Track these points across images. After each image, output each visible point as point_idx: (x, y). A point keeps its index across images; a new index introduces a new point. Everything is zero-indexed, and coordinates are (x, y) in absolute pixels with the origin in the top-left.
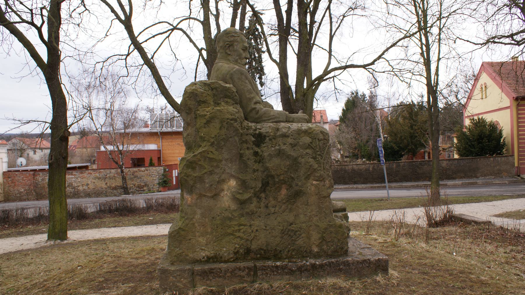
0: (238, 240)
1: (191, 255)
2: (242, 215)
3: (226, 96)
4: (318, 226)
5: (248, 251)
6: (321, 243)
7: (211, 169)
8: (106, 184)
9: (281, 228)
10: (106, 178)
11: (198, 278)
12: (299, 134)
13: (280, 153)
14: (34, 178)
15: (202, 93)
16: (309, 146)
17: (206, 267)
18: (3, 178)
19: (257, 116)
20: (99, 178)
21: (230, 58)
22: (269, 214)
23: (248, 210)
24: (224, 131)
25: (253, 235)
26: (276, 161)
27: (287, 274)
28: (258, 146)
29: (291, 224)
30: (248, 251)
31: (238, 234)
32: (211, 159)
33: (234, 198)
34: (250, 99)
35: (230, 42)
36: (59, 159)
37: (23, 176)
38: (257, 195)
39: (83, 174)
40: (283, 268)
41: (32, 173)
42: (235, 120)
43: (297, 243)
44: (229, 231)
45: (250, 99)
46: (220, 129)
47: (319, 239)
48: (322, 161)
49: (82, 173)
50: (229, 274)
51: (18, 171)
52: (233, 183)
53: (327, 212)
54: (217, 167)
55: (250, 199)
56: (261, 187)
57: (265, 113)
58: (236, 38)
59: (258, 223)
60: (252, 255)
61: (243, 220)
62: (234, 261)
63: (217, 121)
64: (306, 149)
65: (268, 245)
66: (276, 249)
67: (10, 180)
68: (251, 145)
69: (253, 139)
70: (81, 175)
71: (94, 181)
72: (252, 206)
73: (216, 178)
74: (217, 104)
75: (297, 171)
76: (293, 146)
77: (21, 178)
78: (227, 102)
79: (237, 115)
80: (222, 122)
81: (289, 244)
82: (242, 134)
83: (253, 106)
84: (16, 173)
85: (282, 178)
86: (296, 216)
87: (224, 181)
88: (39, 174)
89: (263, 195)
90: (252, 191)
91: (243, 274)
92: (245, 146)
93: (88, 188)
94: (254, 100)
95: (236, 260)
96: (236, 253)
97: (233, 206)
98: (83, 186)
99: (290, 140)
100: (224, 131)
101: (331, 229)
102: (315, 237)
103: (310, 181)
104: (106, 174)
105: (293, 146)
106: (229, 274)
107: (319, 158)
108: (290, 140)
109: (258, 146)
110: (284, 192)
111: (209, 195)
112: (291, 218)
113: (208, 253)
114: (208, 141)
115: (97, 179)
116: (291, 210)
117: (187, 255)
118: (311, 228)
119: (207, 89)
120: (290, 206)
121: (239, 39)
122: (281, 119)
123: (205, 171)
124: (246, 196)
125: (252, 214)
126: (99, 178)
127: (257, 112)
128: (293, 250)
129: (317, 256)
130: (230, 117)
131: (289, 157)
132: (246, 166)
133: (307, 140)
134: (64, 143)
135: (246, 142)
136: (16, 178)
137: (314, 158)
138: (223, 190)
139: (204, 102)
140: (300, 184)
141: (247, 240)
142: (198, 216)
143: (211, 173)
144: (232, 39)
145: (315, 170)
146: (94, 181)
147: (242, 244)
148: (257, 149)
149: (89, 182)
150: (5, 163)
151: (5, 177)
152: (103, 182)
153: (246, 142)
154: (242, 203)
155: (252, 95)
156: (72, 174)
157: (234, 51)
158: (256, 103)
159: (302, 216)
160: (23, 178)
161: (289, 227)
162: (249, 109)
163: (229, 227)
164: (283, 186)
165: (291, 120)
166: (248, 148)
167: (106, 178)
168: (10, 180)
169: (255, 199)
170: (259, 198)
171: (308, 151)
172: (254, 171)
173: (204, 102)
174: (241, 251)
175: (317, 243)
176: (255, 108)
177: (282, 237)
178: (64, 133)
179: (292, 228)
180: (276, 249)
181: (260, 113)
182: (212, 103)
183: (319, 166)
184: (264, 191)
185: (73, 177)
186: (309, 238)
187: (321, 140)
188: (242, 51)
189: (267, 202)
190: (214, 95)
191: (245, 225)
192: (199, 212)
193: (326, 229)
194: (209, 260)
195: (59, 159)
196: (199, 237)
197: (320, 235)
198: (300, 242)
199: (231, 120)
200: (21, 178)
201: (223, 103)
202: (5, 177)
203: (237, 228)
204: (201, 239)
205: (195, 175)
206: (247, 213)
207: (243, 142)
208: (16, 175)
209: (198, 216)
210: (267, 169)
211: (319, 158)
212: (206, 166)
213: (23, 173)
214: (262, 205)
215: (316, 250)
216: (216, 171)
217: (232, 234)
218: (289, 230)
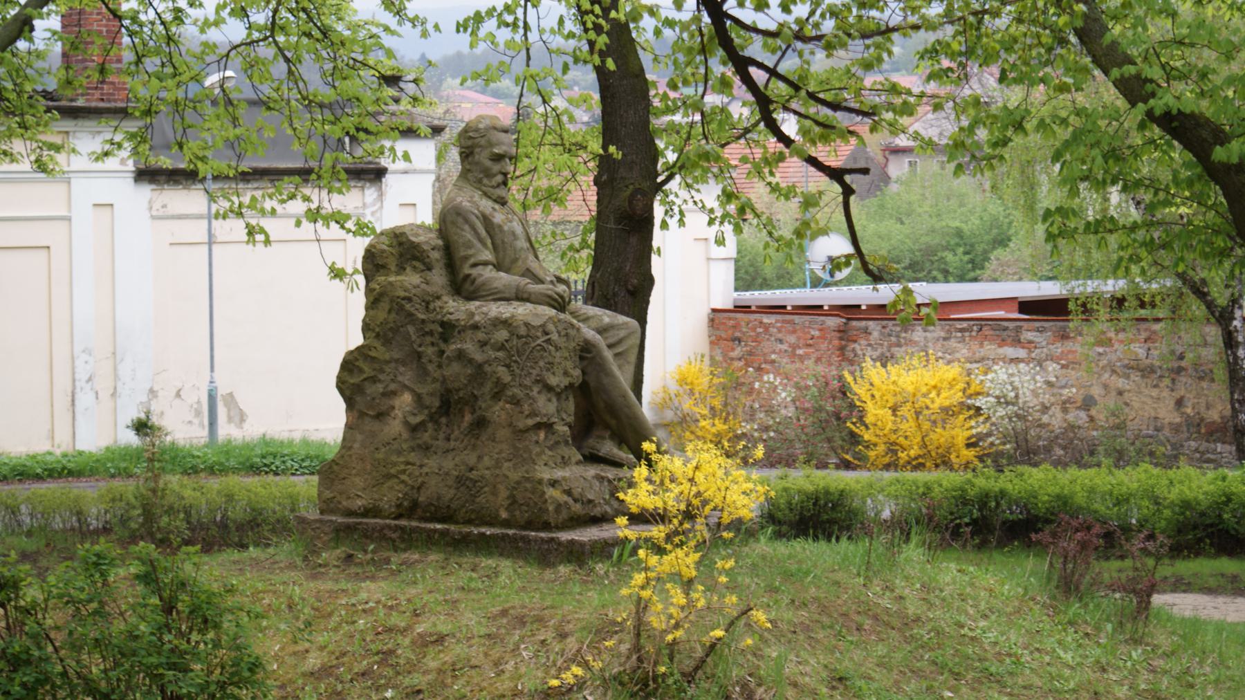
0: (402, 486)
1: (344, 503)
2: (413, 450)
3: (415, 258)
4: (507, 477)
5: (415, 505)
6: (510, 505)
7: (372, 374)
8: (1179, 403)
9: (456, 473)
10: (1180, 370)
11: (342, 534)
12: (495, 326)
13: (461, 355)
14: (842, 349)
15: (383, 251)
16: (502, 347)
17: (352, 520)
18: (712, 343)
19: (472, 288)
20: (1147, 371)
21: (470, 175)
22: (448, 451)
23: (420, 442)
24: (393, 315)
25: (420, 480)
26: (456, 367)
27: (448, 544)
28: (446, 341)
29: (471, 469)
30: (415, 505)
31: (404, 477)
32: (373, 359)
33: (406, 423)
34: (466, 258)
35: (467, 148)
36: (615, 295)
37: (792, 339)
38: (433, 418)
39: (1069, 345)
40: (444, 533)
41: (833, 322)
42: (409, 299)
43: (478, 500)
44: (393, 471)
45: (466, 258)
46: (390, 312)
47: (508, 498)
48: (517, 371)
49: (1064, 337)
50: (376, 534)
51: (778, 309)
52: (407, 398)
53: (525, 456)
54: (382, 371)
55: (422, 423)
56: (440, 407)
57: (484, 284)
58: (477, 141)
59: (432, 463)
60: (419, 511)
61: (413, 457)
62: (395, 518)
63: (387, 299)
64: (499, 350)
65: (439, 498)
66: (448, 507)
67: (737, 352)
68: (435, 339)
69: (440, 330)
70: (1058, 348)
71: (1121, 383)
72: (426, 437)
73: (380, 388)
74: (401, 269)
75: (482, 384)
76: (483, 344)
77: (784, 347)
78: (415, 267)
79: (414, 291)
80: (392, 301)
81: (467, 501)
82: (423, 321)
83: (467, 270)
84: (767, 319)
85: (461, 394)
86: (480, 458)
87: (394, 393)
88: (866, 331)
89: (444, 420)
90: (426, 412)
91: (394, 536)
92: (428, 339)
93: (1092, 419)
94: (472, 261)
95: (399, 517)
96: (399, 506)
97: (405, 435)
98: (1065, 410)
99: (481, 335)
100: (393, 315)
101: (528, 485)
102: (503, 493)
103: (501, 404)
104: (1179, 349)
105: (483, 344)
106: (376, 534)
107: (515, 366)
108: (481, 335)
109: (446, 341)
110: (468, 418)
111: (371, 413)
112: (472, 460)
113: (364, 502)
114: (373, 330)
115: (1137, 377)
116: (474, 447)
117: (340, 503)
118: (499, 480)
119: (395, 243)
120: (473, 441)
121: (483, 142)
122: (507, 295)
123: (365, 376)
124: (418, 419)
125: (426, 449)
126: (1147, 371)
127: (473, 282)
128: (473, 511)
129: (507, 524)
130: (402, 294)
131: (471, 361)
132: (426, 373)
133: (502, 335)
134: (634, 240)
135: (431, 333)
136: (767, 346)
137: (508, 366)
138: (393, 408)
139: (383, 267)
140: (483, 406)
141: (413, 488)
142: (356, 445)
143: (373, 380)
144: (470, 143)
145: (505, 386)
146: (1121, 383)
147: (406, 494)
148: (443, 346)
149: (1096, 391)
150: (723, 264)
151: (720, 338)
152: (1166, 393)
153: (431, 333)
154: (414, 429)
155: (470, 252)
156: (1017, 342)
157: (477, 163)
158: (475, 265)
159: (486, 459)
160: (794, 347)
161: (468, 474)
162: (461, 276)
163: (395, 464)
164: (467, 409)
165: (525, 296)
166: (433, 344)
167: (1180, 370)
168: (737, 352)
169: (430, 425)
170: (436, 422)
171: (500, 354)
172: (435, 380)
173: (383, 267)
174: (406, 504)
175: (506, 503)
176: (468, 276)
177: (457, 489)
178: (630, 202)
179: (474, 475)
180: (448, 507)
181: (479, 281)
182: (393, 268)
183: (513, 380)
184: (447, 414)
185: (1022, 353)
186: (495, 493)
187: (522, 337)
188: (488, 163)
189: (449, 431)
190: (401, 255)
191: (413, 464)
192: (359, 437)
193: (518, 483)
194: (367, 512)
195: (615, 295)
196: (356, 475)
197: (508, 493)
198: (481, 499)
199: (404, 299)
200: (784, 347)
201: (408, 269)
202: (720, 338)
203: (403, 467)
204: (357, 480)
205: (352, 381)
206: (419, 446)
207: (427, 333)
208: (767, 327)
209: (356, 445)
210: (444, 381)
211: (515, 366)
212: (366, 369)
213: (797, 318)
214: (442, 436)
215: (504, 515)
216: (381, 377)
217: (397, 477)
218: (467, 479)
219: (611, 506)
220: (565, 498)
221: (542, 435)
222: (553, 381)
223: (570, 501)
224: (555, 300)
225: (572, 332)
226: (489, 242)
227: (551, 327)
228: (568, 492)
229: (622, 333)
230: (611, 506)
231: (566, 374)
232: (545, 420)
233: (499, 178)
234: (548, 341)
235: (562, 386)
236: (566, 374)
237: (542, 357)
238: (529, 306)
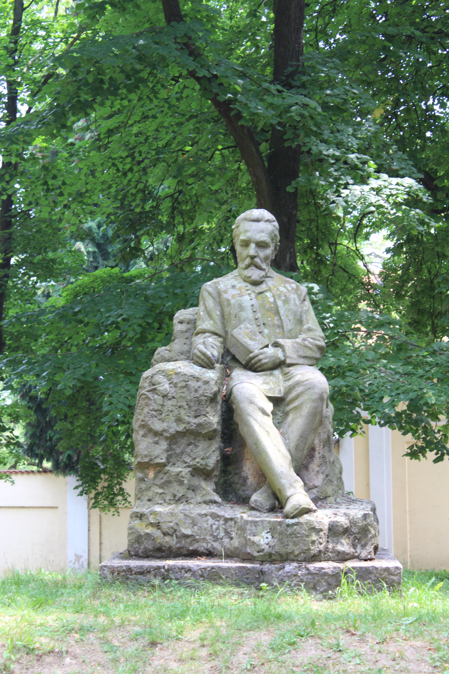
219: (222, 544)
220: (149, 530)
221: (151, 474)
222: (158, 426)
223: (157, 533)
224: (199, 357)
225: (193, 384)
226: (217, 313)
227: (160, 378)
228: (157, 526)
229: (299, 389)
230: (222, 544)
231: (179, 420)
232: (146, 460)
233: (248, 261)
234: (154, 391)
235: (172, 431)
236: (179, 420)
237: (147, 405)
238: (172, 363)
